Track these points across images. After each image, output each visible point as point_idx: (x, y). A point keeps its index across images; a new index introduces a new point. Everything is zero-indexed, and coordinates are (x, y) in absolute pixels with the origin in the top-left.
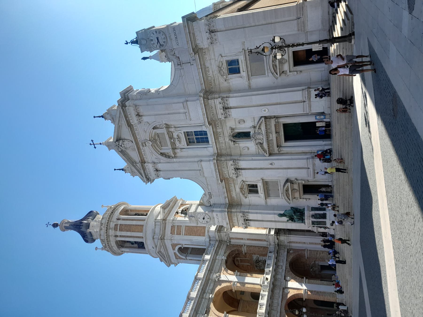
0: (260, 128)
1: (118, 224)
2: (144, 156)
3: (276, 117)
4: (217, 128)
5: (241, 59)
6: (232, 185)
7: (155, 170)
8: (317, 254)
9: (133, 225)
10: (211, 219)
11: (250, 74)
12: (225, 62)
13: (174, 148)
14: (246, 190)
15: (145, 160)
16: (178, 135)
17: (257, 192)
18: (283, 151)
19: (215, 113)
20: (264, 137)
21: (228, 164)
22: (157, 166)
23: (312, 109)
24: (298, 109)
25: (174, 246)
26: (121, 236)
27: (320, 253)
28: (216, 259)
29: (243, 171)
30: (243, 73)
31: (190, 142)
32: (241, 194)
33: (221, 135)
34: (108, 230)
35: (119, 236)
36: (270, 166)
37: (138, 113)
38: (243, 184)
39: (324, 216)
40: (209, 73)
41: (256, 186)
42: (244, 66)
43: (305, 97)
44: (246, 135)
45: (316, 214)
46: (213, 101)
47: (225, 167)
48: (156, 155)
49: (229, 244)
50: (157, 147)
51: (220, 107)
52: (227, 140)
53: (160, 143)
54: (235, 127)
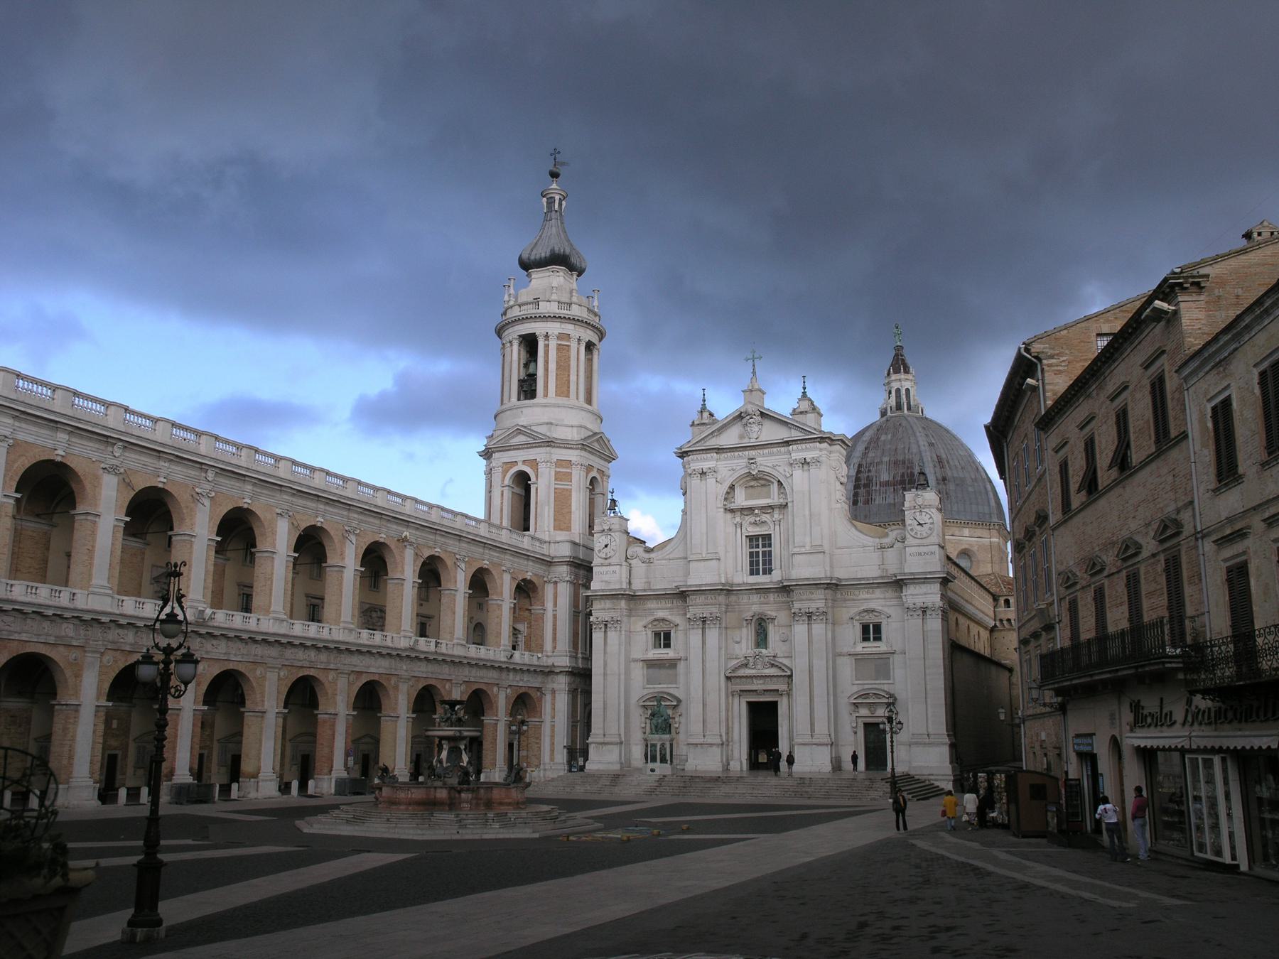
0: (773, 665)
2: (729, 454)
3: (789, 693)
5: (882, 647)
7: (705, 471)
8: (537, 738)
9: (569, 375)
10: (606, 559)
11: (859, 657)
13: (742, 510)
14: (663, 627)
15: (723, 455)
18: (733, 700)
19: (804, 597)
25: (533, 463)
26: (547, 346)
27: (537, 743)
29: (700, 631)
30: (861, 647)
31: (752, 539)
32: (652, 618)
33: (762, 599)
35: (547, 342)
37: (808, 463)
39: (663, 760)
41: (667, 645)
42: (870, 649)
44: (761, 639)
45: (665, 749)
46: (822, 597)
48: (731, 476)
49: (545, 579)
50: (745, 480)
51: (813, 606)
52: (755, 608)
53: (752, 486)
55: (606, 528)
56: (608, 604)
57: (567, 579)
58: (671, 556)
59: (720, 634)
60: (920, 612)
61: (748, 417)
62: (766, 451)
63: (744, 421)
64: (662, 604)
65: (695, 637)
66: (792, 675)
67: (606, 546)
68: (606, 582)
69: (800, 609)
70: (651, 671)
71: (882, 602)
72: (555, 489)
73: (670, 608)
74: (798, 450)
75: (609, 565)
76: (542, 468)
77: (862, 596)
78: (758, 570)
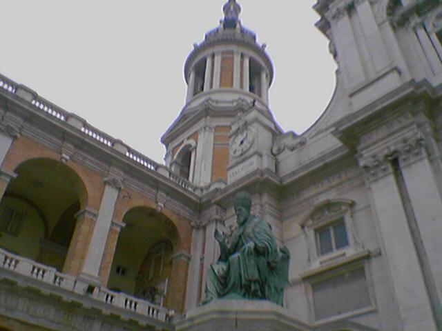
14: (328, 217)
17: (324, 249)
21: (406, 131)
28: (158, 189)
29: (392, 179)
32: (312, 209)
38: (343, 208)
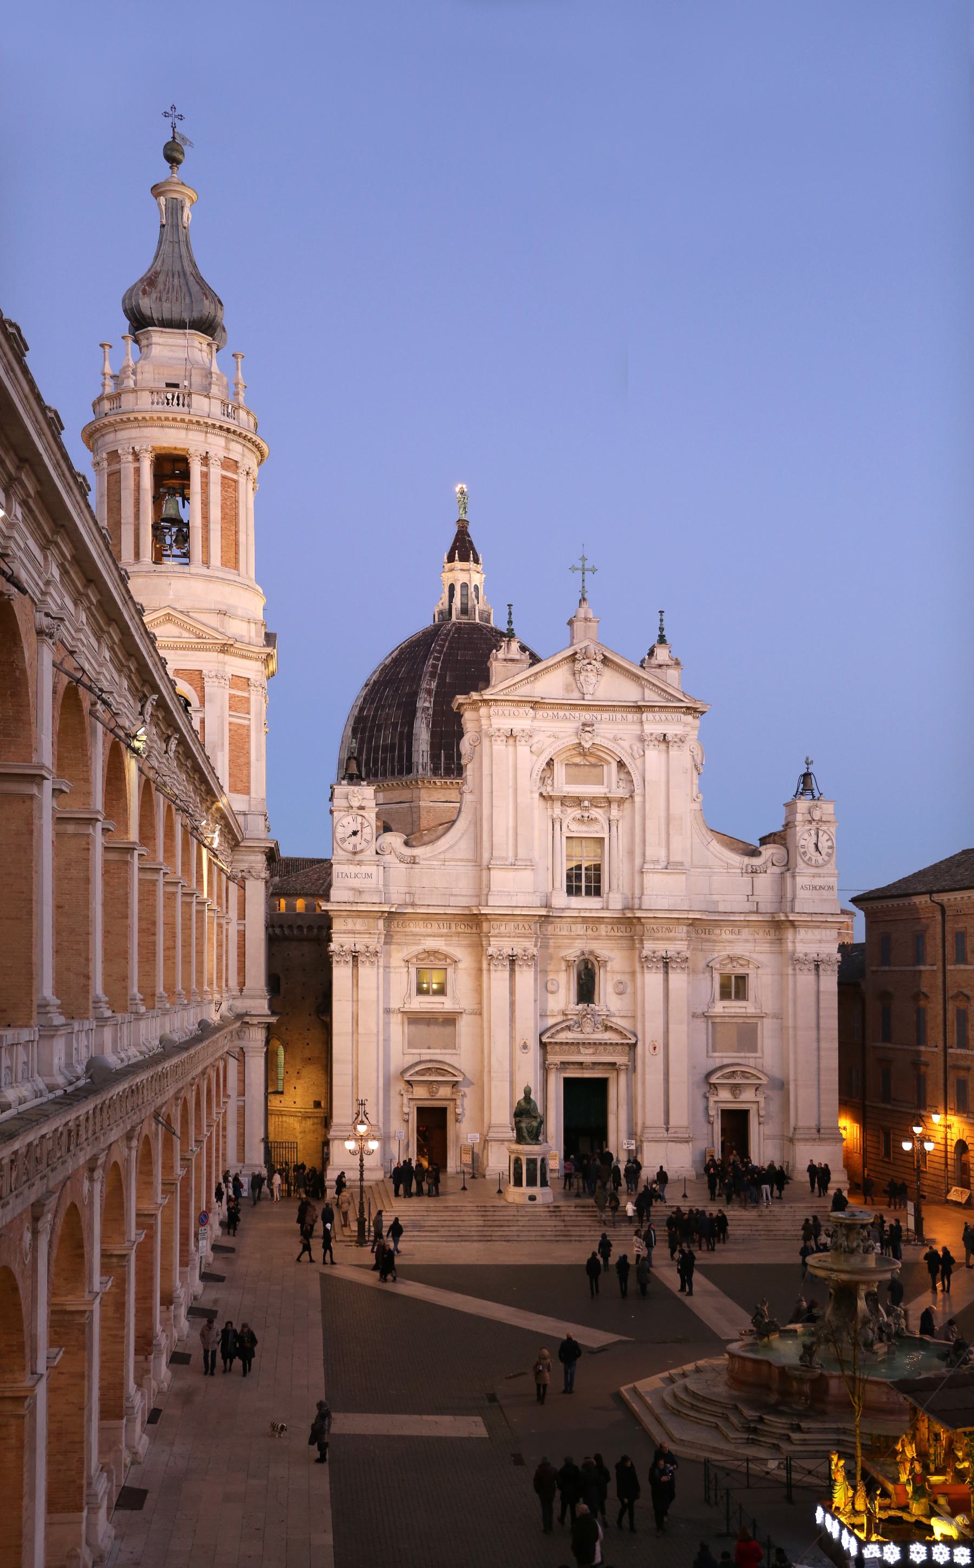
0: (607, 1028)
1: (237, 473)
2: (550, 713)
3: (632, 1068)
4: (610, 927)
6: (445, 931)
12: (747, 972)
16: (596, 819)
20: (587, 1036)
22: (523, 743)
23: (652, 1144)
24: (651, 1114)
26: (205, 476)
29: (507, 974)
30: (720, 1007)
32: (419, 948)
34: (224, 434)
36: (519, 1042)
38: (448, 960)
40: (728, 932)
42: (733, 1010)
43: (676, 1132)
46: (684, 935)
47: (517, 931)
51: (671, 948)
53: (576, 765)
54: (608, 969)
55: (355, 803)
56: (359, 925)
57: (263, 875)
58: (448, 855)
59: (536, 980)
60: (812, 967)
61: (587, 661)
62: (606, 715)
63: (578, 666)
64: (434, 928)
65: (498, 979)
66: (635, 1045)
67: (355, 833)
68: (353, 889)
69: (654, 952)
70: (413, 1028)
71: (750, 946)
72: (230, 723)
73: (446, 936)
74: (654, 721)
75: (360, 863)
76: (210, 687)
77: (724, 936)
78: (579, 889)
